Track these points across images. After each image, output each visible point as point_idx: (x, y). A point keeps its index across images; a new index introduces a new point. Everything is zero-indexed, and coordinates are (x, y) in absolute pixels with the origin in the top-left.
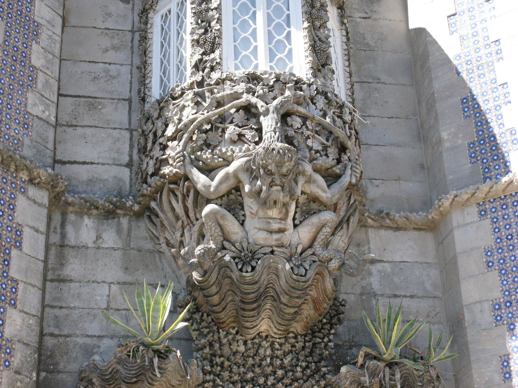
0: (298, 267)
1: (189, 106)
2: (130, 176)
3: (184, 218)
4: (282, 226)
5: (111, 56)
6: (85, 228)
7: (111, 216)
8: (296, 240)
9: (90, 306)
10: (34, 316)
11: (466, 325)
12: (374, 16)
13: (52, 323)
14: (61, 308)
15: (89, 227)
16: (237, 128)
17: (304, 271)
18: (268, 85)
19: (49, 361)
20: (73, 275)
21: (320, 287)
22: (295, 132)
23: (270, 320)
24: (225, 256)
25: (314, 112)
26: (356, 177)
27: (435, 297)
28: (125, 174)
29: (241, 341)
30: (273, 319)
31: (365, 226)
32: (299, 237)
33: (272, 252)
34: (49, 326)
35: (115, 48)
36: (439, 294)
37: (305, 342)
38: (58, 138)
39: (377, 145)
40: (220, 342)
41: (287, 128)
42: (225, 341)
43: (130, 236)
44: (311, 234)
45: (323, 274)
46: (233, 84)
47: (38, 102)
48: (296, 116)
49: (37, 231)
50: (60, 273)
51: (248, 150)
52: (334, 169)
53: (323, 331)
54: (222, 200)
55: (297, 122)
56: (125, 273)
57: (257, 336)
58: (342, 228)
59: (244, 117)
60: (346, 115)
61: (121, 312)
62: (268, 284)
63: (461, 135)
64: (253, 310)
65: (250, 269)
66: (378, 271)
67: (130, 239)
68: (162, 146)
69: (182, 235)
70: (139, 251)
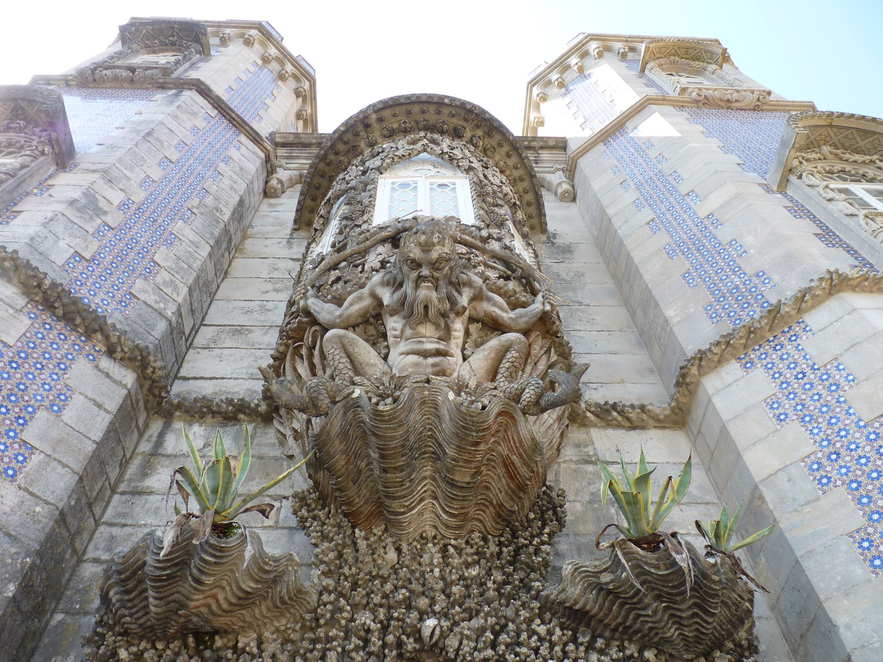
0: (472, 402)
4: (442, 347)
5: (272, 296)
7: (232, 423)
10: (47, 503)
12: (567, 261)
13: (102, 545)
14: (124, 525)
15: (197, 434)
17: (480, 406)
19: (77, 597)
20: (156, 486)
23: (434, 502)
24: (353, 392)
27: (707, 503)
29: (390, 544)
31: (585, 425)
33: (428, 381)
34: (97, 549)
35: (276, 290)
37: (500, 544)
38: (187, 358)
42: (362, 544)
44: (490, 361)
47: (150, 291)
49: (100, 406)
50: (139, 484)
54: (355, 330)
63: (691, 305)
65: (389, 400)
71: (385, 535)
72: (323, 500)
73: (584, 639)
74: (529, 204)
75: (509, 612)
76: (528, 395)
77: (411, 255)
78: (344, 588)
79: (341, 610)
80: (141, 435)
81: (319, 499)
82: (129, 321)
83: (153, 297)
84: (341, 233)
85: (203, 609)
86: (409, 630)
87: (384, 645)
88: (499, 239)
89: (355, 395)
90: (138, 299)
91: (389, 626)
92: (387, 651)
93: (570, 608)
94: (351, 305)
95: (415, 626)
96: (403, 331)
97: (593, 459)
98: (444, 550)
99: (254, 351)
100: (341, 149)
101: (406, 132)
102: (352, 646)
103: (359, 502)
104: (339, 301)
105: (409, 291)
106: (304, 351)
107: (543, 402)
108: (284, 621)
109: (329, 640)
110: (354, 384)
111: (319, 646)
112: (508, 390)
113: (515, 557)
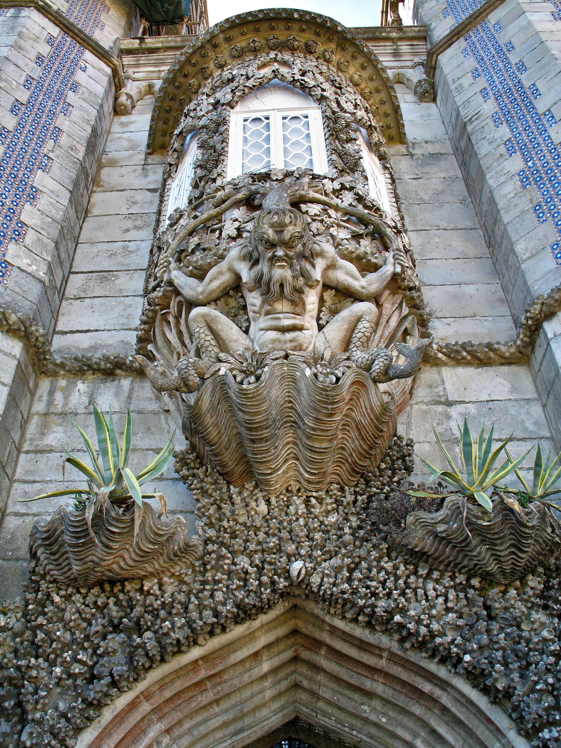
0: (326, 375)
3: (180, 349)
5: (132, 235)
6: (77, 393)
7: (111, 378)
8: (322, 344)
9: (71, 479)
15: (82, 391)
17: (334, 379)
18: (277, 180)
24: (219, 369)
26: (402, 266)
29: (261, 498)
33: (286, 357)
40: (233, 504)
42: (237, 500)
47: (22, 255)
50: (39, 443)
65: (252, 379)
71: (256, 491)
72: (200, 459)
73: (423, 572)
74: (386, 115)
75: (362, 552)
76: (378, 366)
77: (265, 236)
78: (224, 538)
79: (224, 557)
80: (33, 395)
81: (197, 457)
82: (8, 291)
83: (25, 261)
84: (196, 186)
85: (115, 566)
86: (279, 571)
87: (261, 584)
88: (351, 189)
89: (222, 372)
90: (13, 265)
91: (263, 568)
92: (262, 589)
93: (412, 550)
94: (211, 281)
95: (285, 568)
96: (261, 307)
97: (443, 399)
98: (307, 502)
99: (122, 299)
100: (190, 71)
101: (255, 51)
102: (234, 587)
103: (231, 465)
104: (200, 274)
105: (265, 271)
106: (171, 319)
107: (391, 373)
108: (178, 568)
109: (217, 582)
110: (220, 361)
111: (208, 587)
112: (360, 360)
113: (368, 503)
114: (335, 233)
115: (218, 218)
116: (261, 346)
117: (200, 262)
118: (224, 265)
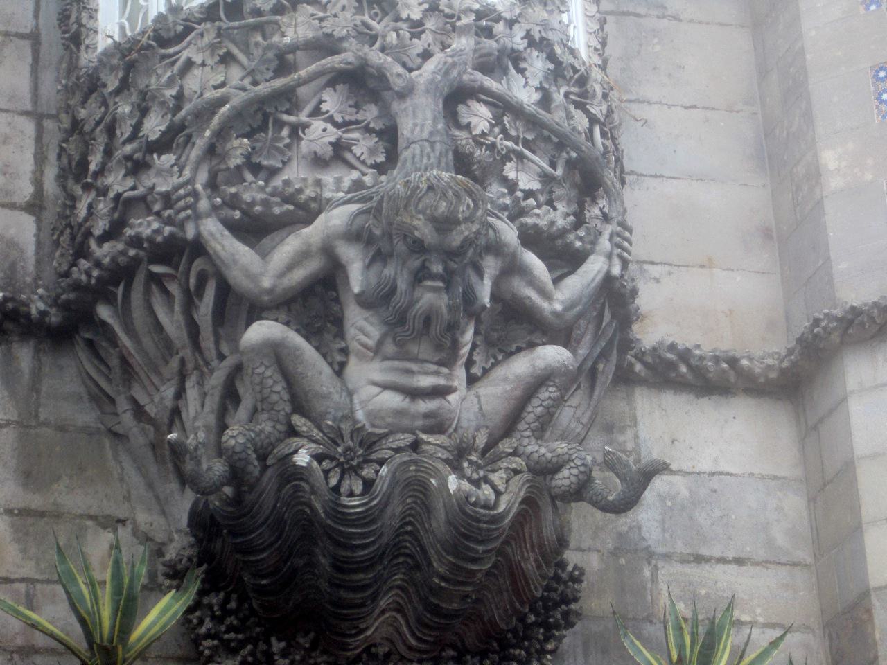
0: (476, 483)
1: (203, 64)
2: (37, 236)
3: (187, 353)
4: (442, 381)
8: (472, 417)
11: (878, 636)
16: (330, 127)
17: (493, 497)
18: (408, 19)
21: (527, 536)
22: (474, 141)
23: (399, 616)
24: (296, 452)
25: (524, 93)
27: (795, 564)
28: (24, 230)
30: (411, 613)
32: (481, 409)
33: (415, 446)
36: (803, 555)
39: (655, 176)
41: (457, 133)
43: (38, 391)
45: (537, 504)
46: (321, 14)
48: (479, 101)
51: (358, 185)
52: (571, 237)
53: (526, 643)
55: (479, 116)
56: (25, 485)
57: (364, 656)
58: (578, 387)
59: (348, 98)
60: (596, 101)
61: (17, 585)
62: (401, 527)
63: (870, 162)
64: (364, 588)
65: (358, 487)
66: (659, 495)
67: (38, 398)
68: (129, 164)
69: (180, 393)
70: (62, 429)
76: (565, 479)
77: (416, 233)
94: (290, 268)
96: (380, 343)
104: (255, 229)
105: (402, 285)
112: (536, 456)
114: (512, 175)
115: (288, 98)
116: (371, 415)
117: (258, 208)
118: (313, 233)
